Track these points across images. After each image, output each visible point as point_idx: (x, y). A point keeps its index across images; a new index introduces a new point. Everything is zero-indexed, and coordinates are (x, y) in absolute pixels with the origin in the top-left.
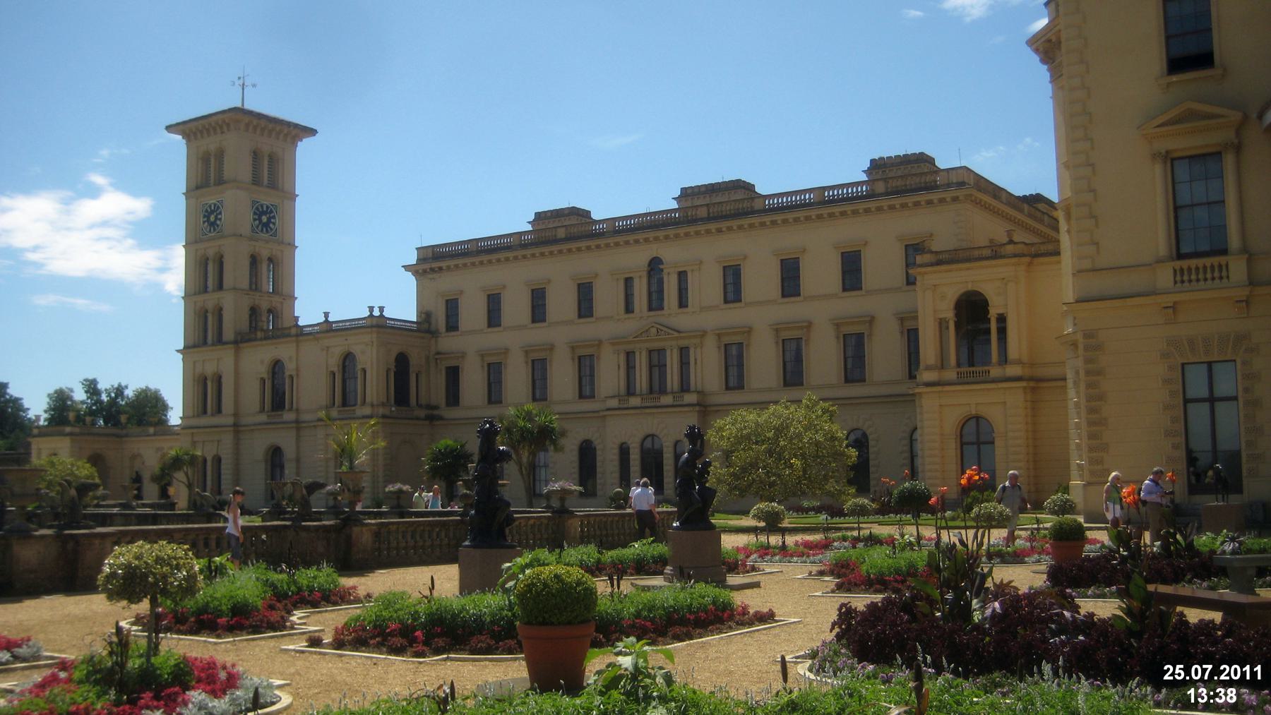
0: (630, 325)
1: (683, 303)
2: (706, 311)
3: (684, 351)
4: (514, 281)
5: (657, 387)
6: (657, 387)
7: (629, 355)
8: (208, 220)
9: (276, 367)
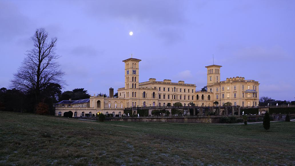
0: (173, 93)
1: (177, 91)
2: (178, 93)
3: (177, 96)
4: (162, 87)
5: (175, 99)
6: (175, 99)
7: (173, 96)
9: (144, 93)
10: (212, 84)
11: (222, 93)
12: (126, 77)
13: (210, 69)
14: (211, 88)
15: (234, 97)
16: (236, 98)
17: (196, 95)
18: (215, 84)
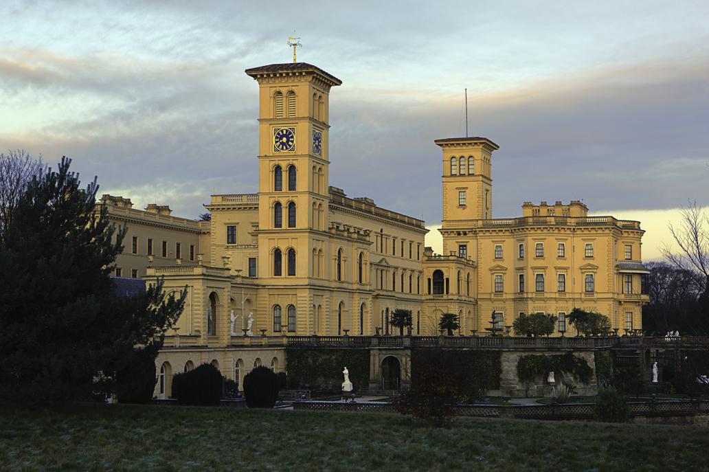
8: (284, 136)
10: (470, 225)
11: (534, 268)
12: (269, 166)
13: (457, 152)
14: (462, 239)
15: (584, 291)
16: (596, 296)
17: (429, 273)
18: (485, 226)
